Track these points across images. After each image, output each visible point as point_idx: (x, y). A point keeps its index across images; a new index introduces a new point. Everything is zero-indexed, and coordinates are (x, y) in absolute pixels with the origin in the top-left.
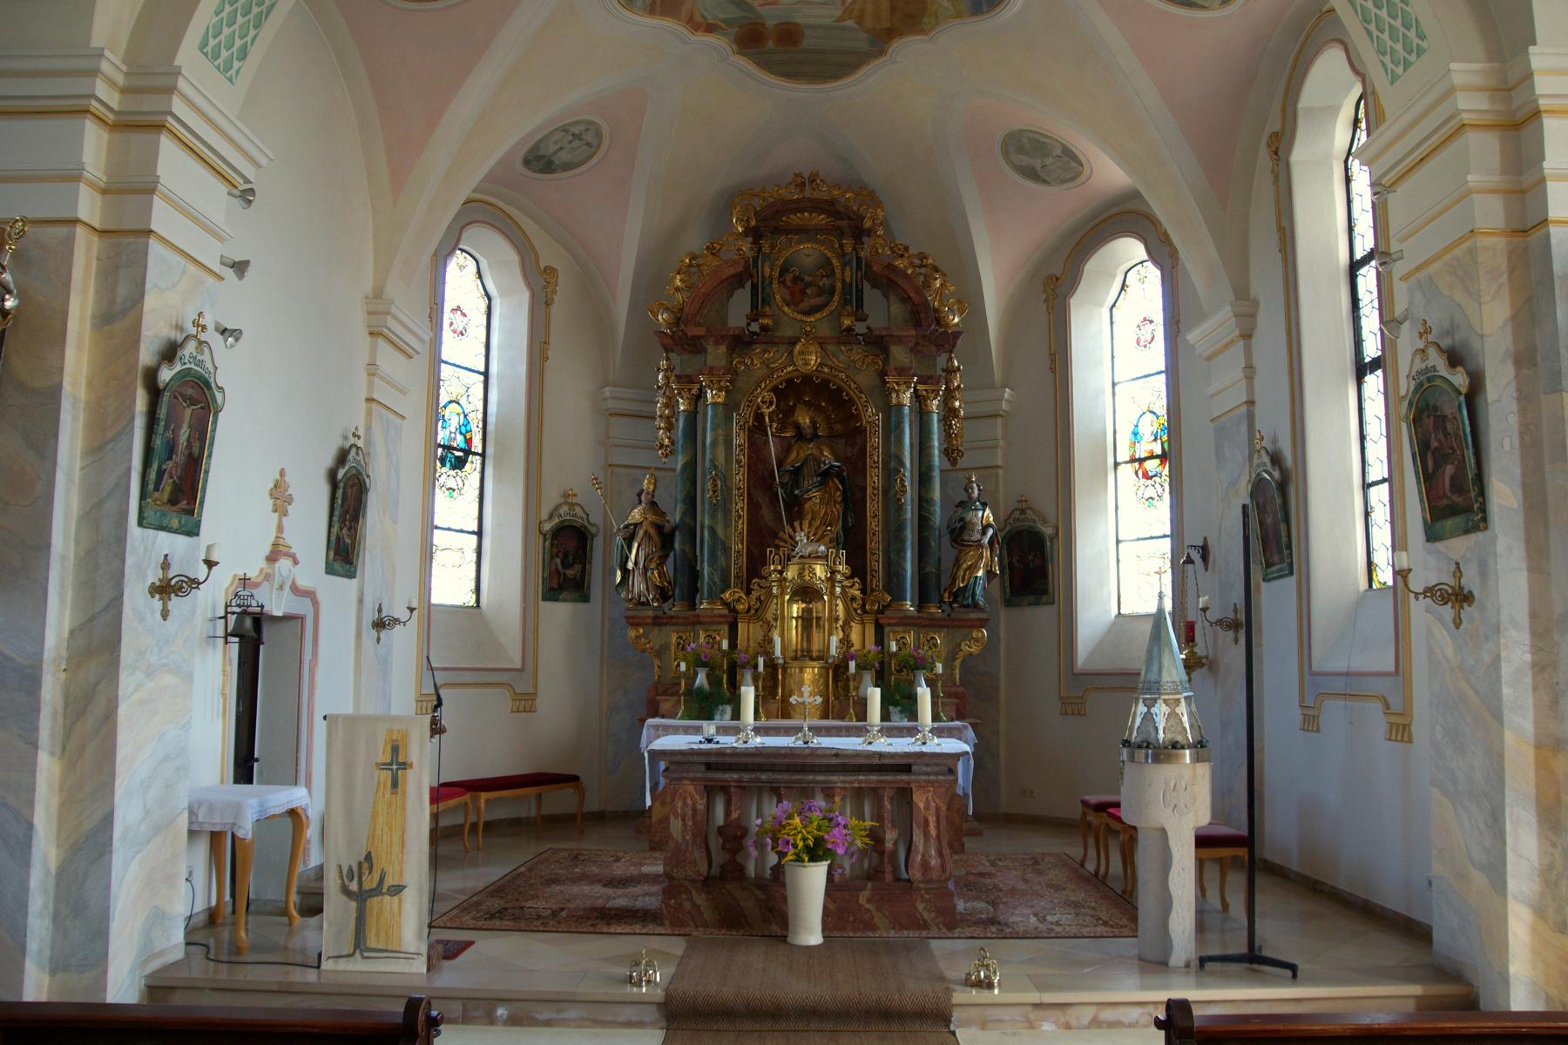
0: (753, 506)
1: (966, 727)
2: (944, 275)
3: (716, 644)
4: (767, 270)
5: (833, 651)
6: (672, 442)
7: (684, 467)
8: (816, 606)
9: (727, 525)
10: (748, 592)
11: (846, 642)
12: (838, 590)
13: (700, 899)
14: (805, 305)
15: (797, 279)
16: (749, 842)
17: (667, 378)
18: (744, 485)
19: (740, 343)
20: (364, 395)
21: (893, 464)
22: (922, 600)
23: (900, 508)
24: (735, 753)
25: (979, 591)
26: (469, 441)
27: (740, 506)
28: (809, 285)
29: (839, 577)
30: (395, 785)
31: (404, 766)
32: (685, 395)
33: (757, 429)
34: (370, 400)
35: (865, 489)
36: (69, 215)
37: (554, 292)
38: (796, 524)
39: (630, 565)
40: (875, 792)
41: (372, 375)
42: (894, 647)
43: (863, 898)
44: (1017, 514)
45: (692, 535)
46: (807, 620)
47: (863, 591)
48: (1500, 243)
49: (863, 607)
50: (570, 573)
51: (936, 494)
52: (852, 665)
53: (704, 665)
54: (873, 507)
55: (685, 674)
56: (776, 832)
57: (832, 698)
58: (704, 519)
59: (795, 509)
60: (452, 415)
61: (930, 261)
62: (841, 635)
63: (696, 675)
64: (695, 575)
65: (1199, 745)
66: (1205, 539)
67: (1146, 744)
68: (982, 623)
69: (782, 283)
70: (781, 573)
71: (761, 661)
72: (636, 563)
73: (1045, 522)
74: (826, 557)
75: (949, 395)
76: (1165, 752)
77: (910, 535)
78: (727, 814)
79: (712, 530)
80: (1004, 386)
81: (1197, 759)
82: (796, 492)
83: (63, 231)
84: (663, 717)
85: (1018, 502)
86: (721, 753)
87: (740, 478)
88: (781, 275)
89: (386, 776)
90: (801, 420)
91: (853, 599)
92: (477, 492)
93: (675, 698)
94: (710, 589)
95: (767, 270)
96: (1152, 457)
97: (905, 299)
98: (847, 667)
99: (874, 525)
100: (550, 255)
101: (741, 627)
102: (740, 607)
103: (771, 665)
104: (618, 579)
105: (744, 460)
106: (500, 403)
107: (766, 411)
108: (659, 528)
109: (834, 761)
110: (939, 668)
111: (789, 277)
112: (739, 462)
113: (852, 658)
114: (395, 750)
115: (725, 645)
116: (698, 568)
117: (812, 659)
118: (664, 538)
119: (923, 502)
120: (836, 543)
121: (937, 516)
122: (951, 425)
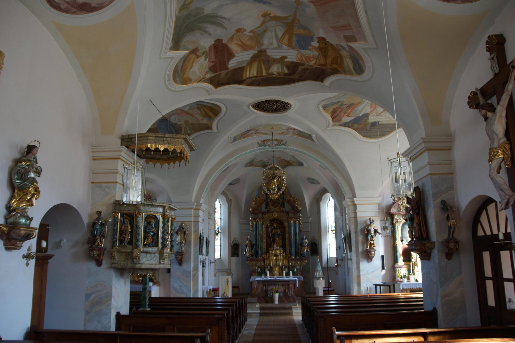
0: (267, 240)
1: (301, 277)
2: (298, 201)
3: (261, 264)
4: (268, 200)
5: (281, 265)
6: (253, 229)
7: (255, 234)
8: (278, 257)
9: (263, 244)
10: (266, 255)
11: (283, 263)
12: (281, 255)
13: (262, 299)
14: (274, 206)
15: (273, 201)
16: (269, 292)
17: (252, 219)
18: (265, 237)
19: (264, 213)
20: (208, 228)
21: (290, 233)
22: (295, 256)
23: (291, 241)
24: (266, 280)
25: (305, 254)
26: (218, 230)
27: (265, 241)
28: (275, 202)
29: (281, 253)
30: (227, 284)
31: (229, 282)
32: (255, 222)
33: (267, 227)
34: (209, 229)
35: (285, 237)
36: (191, 221)
37: (231, 203)
38: (274, 244)
39: (246, 251)
40: (285, 285)
41: (209, 225)
42: (291, 264)
43: (284, 298)
44: (312, 240)
45: (256, 246)
46: (276, 260)
47: (286, 254)
48: (353, 219)
49: (286, 257)
50: (236, 252)
51: (298, 238)
52: (284, 267)
53: (260, 267)
54: (287, 240)
55: (257, 269)
56: (272, 289)
57: (281, 272)
58: (259, 243)
59: (274, 241)
60: (216, 227)
61: (295, 198)
62: (282, 262)
63: (258, 269)
64: (257, 252)
65: (323, 278)
66: (340, 246)
67: (316, 278)
68: (306, 259)
69: (271, 202)
70: (272, 252)
71: (269, 267)
72: (247, 250)
73: (317, 241)
74: (279, 249)
75: (299, 221)
76: (319, 278)
77: (293, 245)
78: (266, 288)
79: (260, 245)
80: (310, 218)
81: (322, 279)
82: (274, 238)
83: (191, 222)
84: (253, 276)
85: (313, 238)
86: (265, 280)
87: (265, 236)
88: (270, 201)
89: (226, 283)
90: (274, 225)
91: (284, 256)
92: (220, 239)
93: (255, 273)
94: (260, 255)
95: (268, 200)
96: (334, 230)
97: (291, 205)
98: (283, 268)
99: (287, 243)
100: (231, 197)
101: (265, 261)
102: (265, 258)
103: (271, 267)
104: (244, 253)
105: (265, 233)
106: (223, 223)
107: (269, 225)
108: (251, 244)
109: (279, 281)
110: (298, 267)
111: (272, 201)
112: (264, 233)
113: (284, 266)
114: (227, 280)
115: (263, 264)
116: (258, 251)
117: (277, 266)
118: (252, 246)
119: (296, 239)
120: (280, 247)
121: (298, 241)
122: (300, 226)
